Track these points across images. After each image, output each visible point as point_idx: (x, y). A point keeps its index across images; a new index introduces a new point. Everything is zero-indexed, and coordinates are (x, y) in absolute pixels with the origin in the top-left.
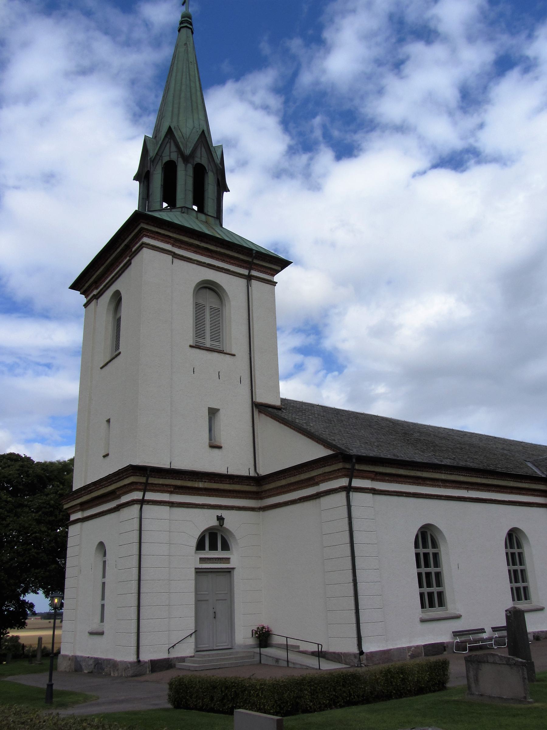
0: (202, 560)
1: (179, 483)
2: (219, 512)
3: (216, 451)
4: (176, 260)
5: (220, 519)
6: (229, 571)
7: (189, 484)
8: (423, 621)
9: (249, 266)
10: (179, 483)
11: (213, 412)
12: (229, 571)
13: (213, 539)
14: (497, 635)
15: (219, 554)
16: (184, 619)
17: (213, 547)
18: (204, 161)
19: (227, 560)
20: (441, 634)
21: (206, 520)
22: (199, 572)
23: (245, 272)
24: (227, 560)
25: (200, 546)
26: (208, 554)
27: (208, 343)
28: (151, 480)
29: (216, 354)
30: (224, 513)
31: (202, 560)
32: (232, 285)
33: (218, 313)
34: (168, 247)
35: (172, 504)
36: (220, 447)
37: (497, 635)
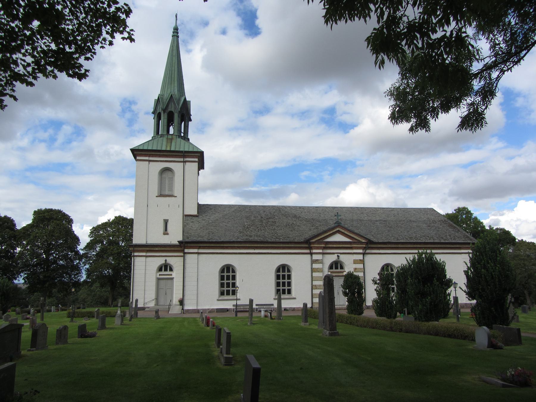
0: (160, 275)
1: (148, 249)
2: (165, 258)
3: (166, 236)
4: (151, 163)
5: (166, 261)
6: (172, 279)
7: (152, 249)
8: (218, 300)
9: (184, 157)
10: (148, 249)
11: (166, 222)
12: (172, 279)
13: (166, 267)
14: (257, 307)
15: (168, 272)
16: (151, 294)
17: (166, 270)
18: (173, 110)
19: (171, 275)
20: (229, 305)
21: (160, 261)
22: (158, 279)
23: (182, 160)
24: (171, 275)
25: (160, 269)
26: (163, 272)
27: (167, 193)
28: (135, 249)
29: (168, 198)
30: (167, 258)
31: (160, 275)
32: (177, 167)
33: (172, 180)
34: (147, 158)
35: (146, 256)
36: (168, 234)
37: (257, 307)
